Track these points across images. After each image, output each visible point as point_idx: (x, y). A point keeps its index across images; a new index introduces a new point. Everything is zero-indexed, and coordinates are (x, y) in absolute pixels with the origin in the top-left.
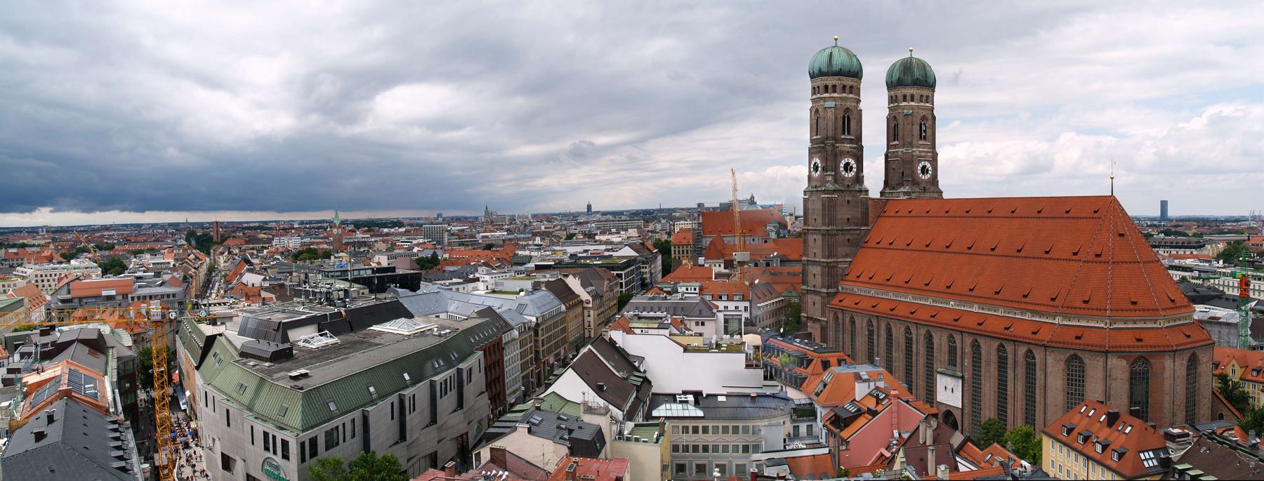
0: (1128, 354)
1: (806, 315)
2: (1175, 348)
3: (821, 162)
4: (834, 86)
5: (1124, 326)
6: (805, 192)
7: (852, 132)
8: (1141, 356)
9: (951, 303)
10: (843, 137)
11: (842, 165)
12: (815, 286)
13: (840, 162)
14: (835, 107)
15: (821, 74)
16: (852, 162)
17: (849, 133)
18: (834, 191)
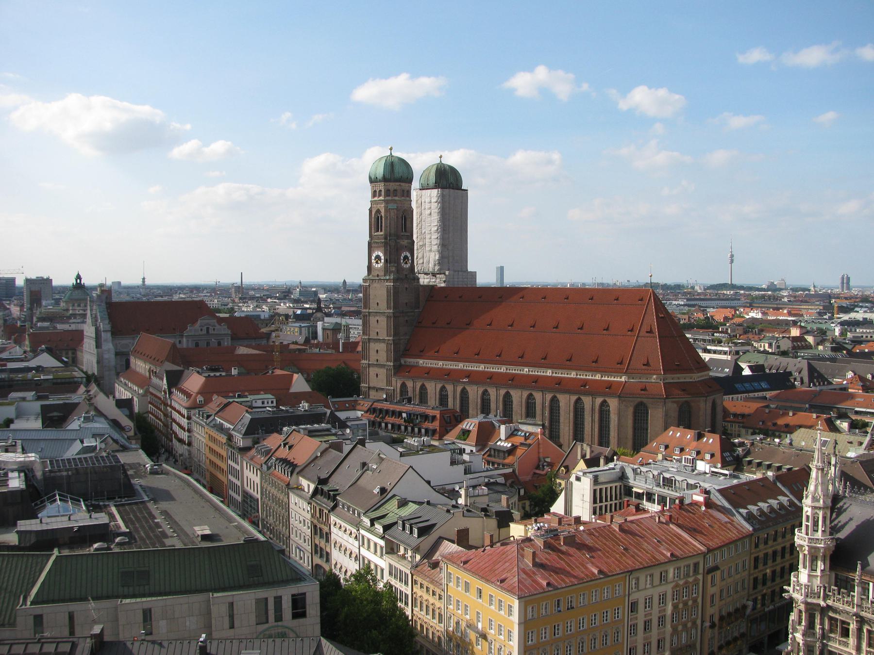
0: (677, 400)
1: (367, 385)
2: (706, 395)
3: (385, 255)
4: (395, 190)
5: (672, 381)
6: (365, 280)
7: (407, 229)
8: (686, 402)
9: (525, 370)
10: (402, 234)
11: (402, 258)
12: (377, 360)
13: (401, 255)
14: (397, 209)
15: (385, 179)
16: (409, 255)
17: (405, 231)
18: (397, 279)
